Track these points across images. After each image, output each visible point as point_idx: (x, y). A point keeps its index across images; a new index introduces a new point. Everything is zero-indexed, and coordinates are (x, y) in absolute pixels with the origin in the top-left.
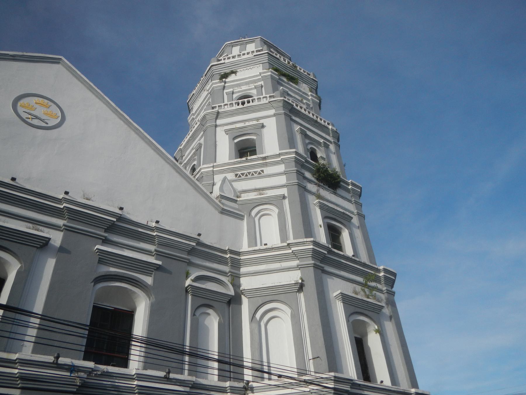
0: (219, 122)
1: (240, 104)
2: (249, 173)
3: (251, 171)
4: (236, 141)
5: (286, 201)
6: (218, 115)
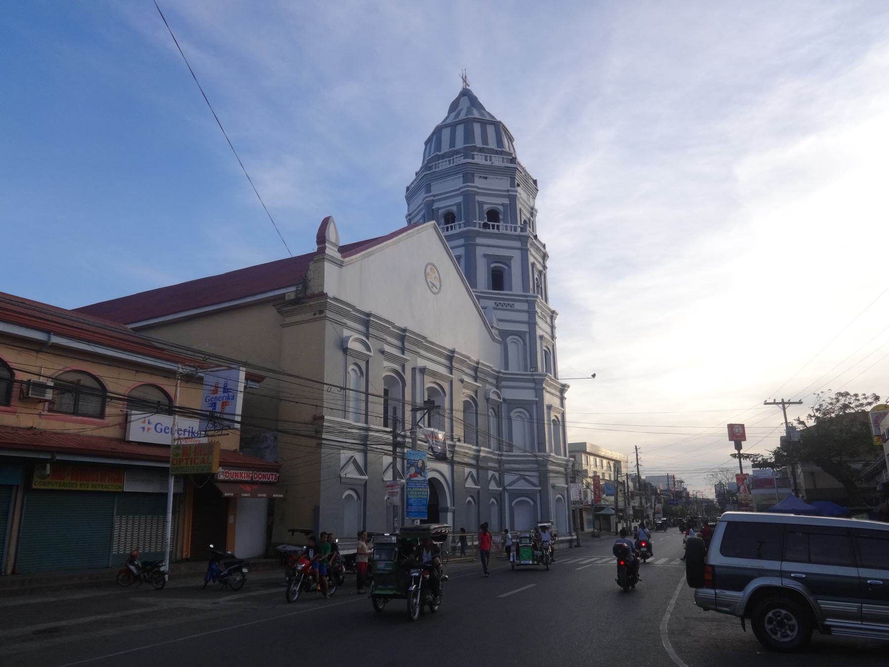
0: (479, 240)
1: (496, 228)
2: (504, 304)
3: (506, 302)
4: (492, 265)
5: (527, 336)
6: (479, 234)
